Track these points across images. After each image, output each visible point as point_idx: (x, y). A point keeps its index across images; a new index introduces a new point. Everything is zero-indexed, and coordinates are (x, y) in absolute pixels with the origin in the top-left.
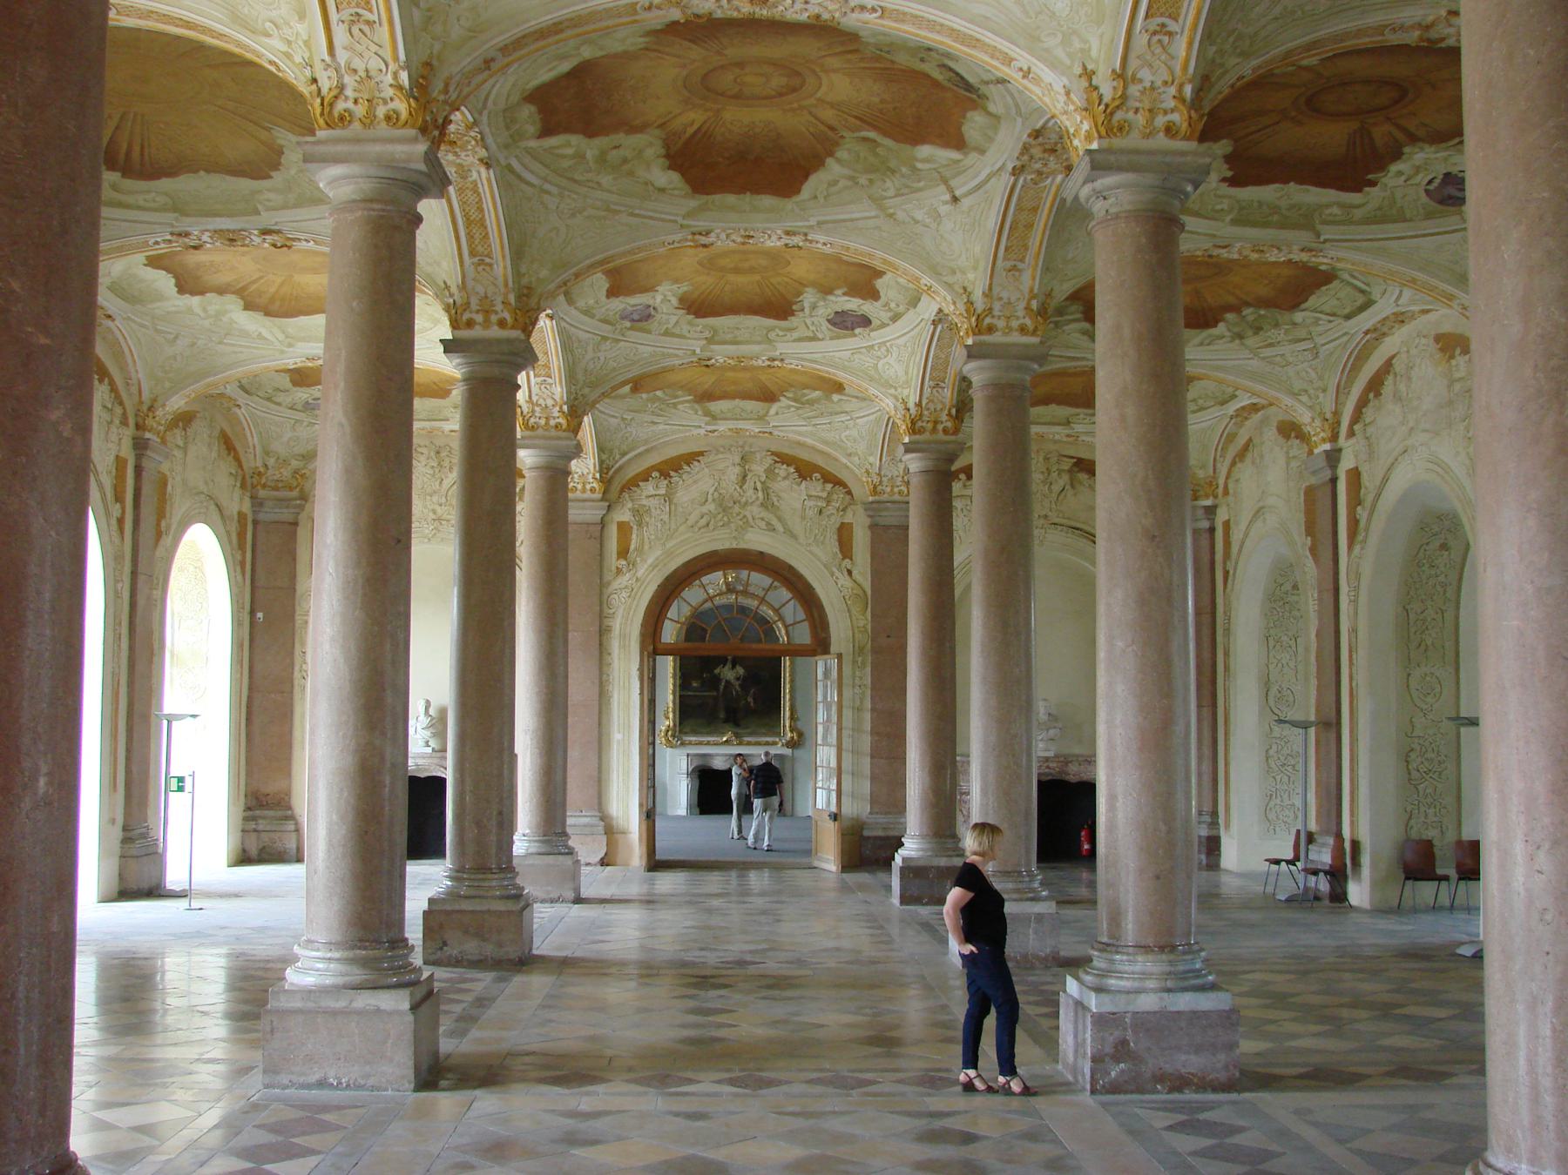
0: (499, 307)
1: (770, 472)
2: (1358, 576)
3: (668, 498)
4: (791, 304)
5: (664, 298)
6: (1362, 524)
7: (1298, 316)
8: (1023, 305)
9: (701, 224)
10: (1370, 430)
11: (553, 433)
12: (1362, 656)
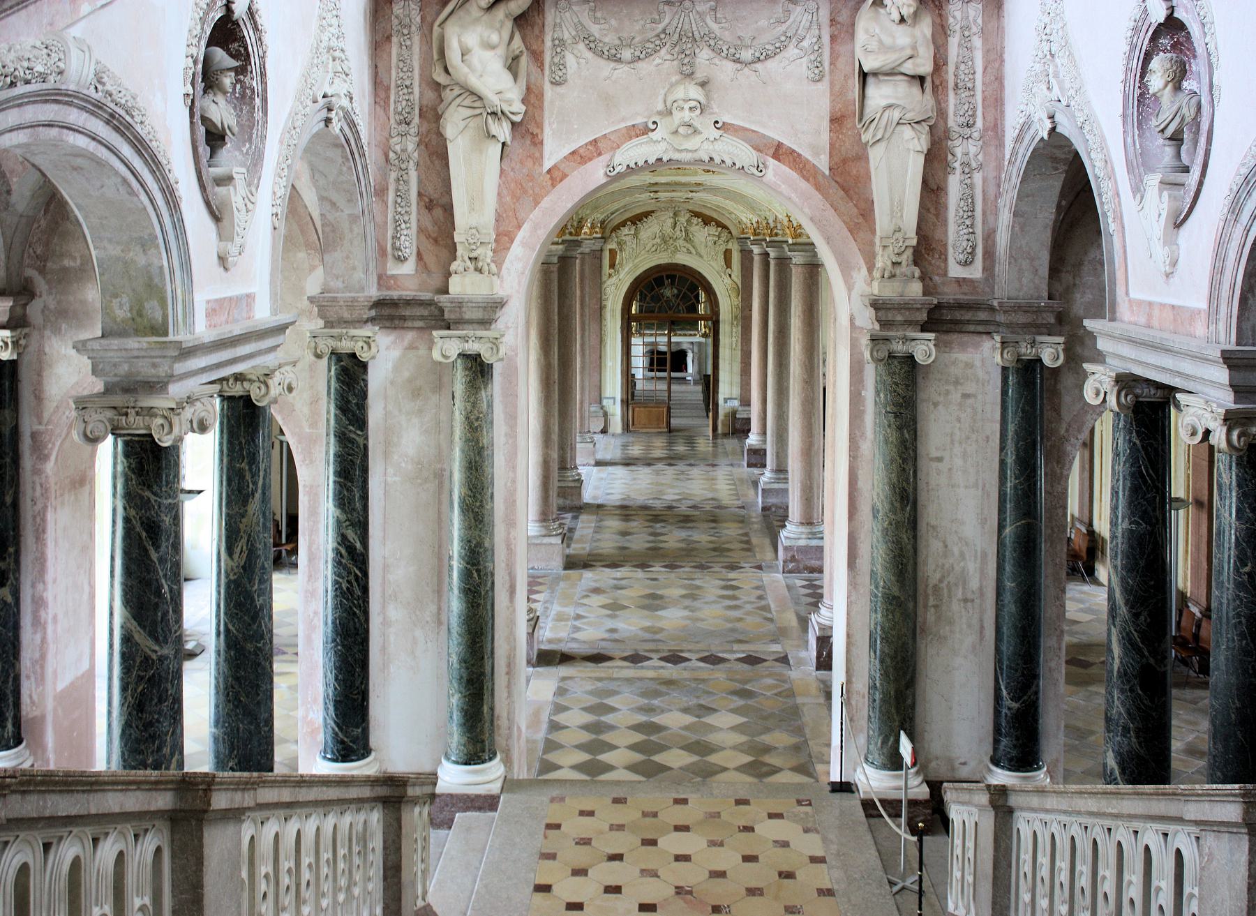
1: (688, 221)
3: (636, 236)
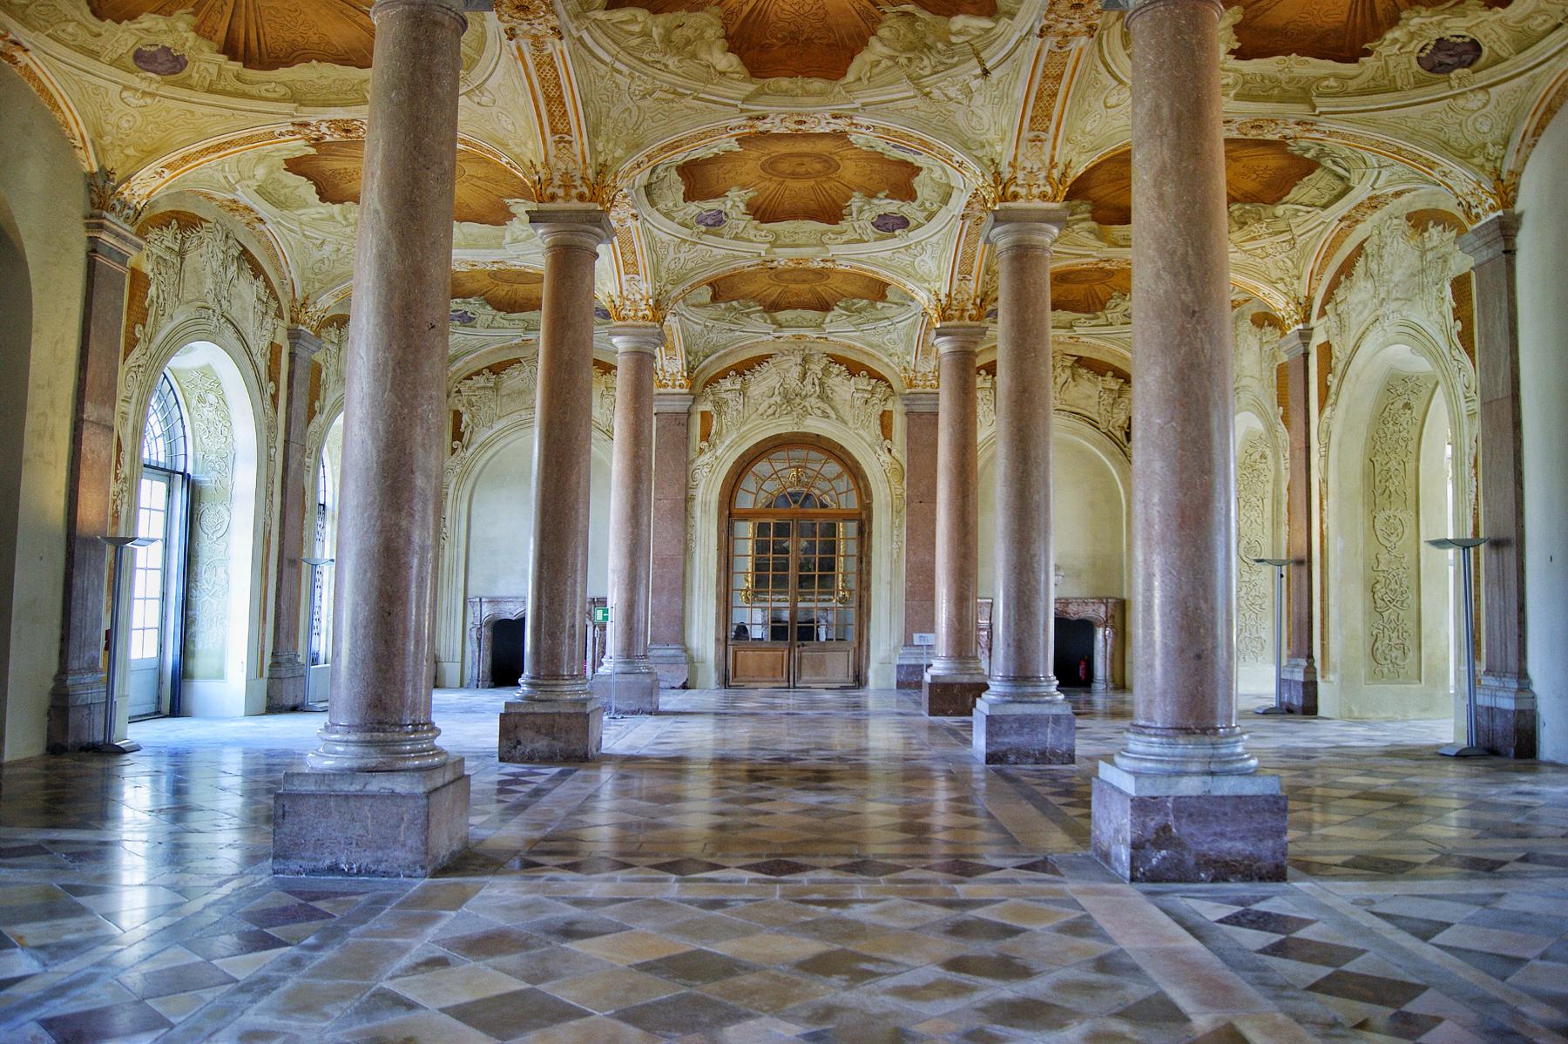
0: (578, 183)
1: (825, 370)
2: (1329, 434)
3: (743, 392)
4: (841, 208)
5: (734, 202)
6: (1333, 390)
7: (1280, 210)
8: (1043, 174)
9: (757, 109)
10: (1341, 308)
11: (641, 323)
12: (1331, 503)
